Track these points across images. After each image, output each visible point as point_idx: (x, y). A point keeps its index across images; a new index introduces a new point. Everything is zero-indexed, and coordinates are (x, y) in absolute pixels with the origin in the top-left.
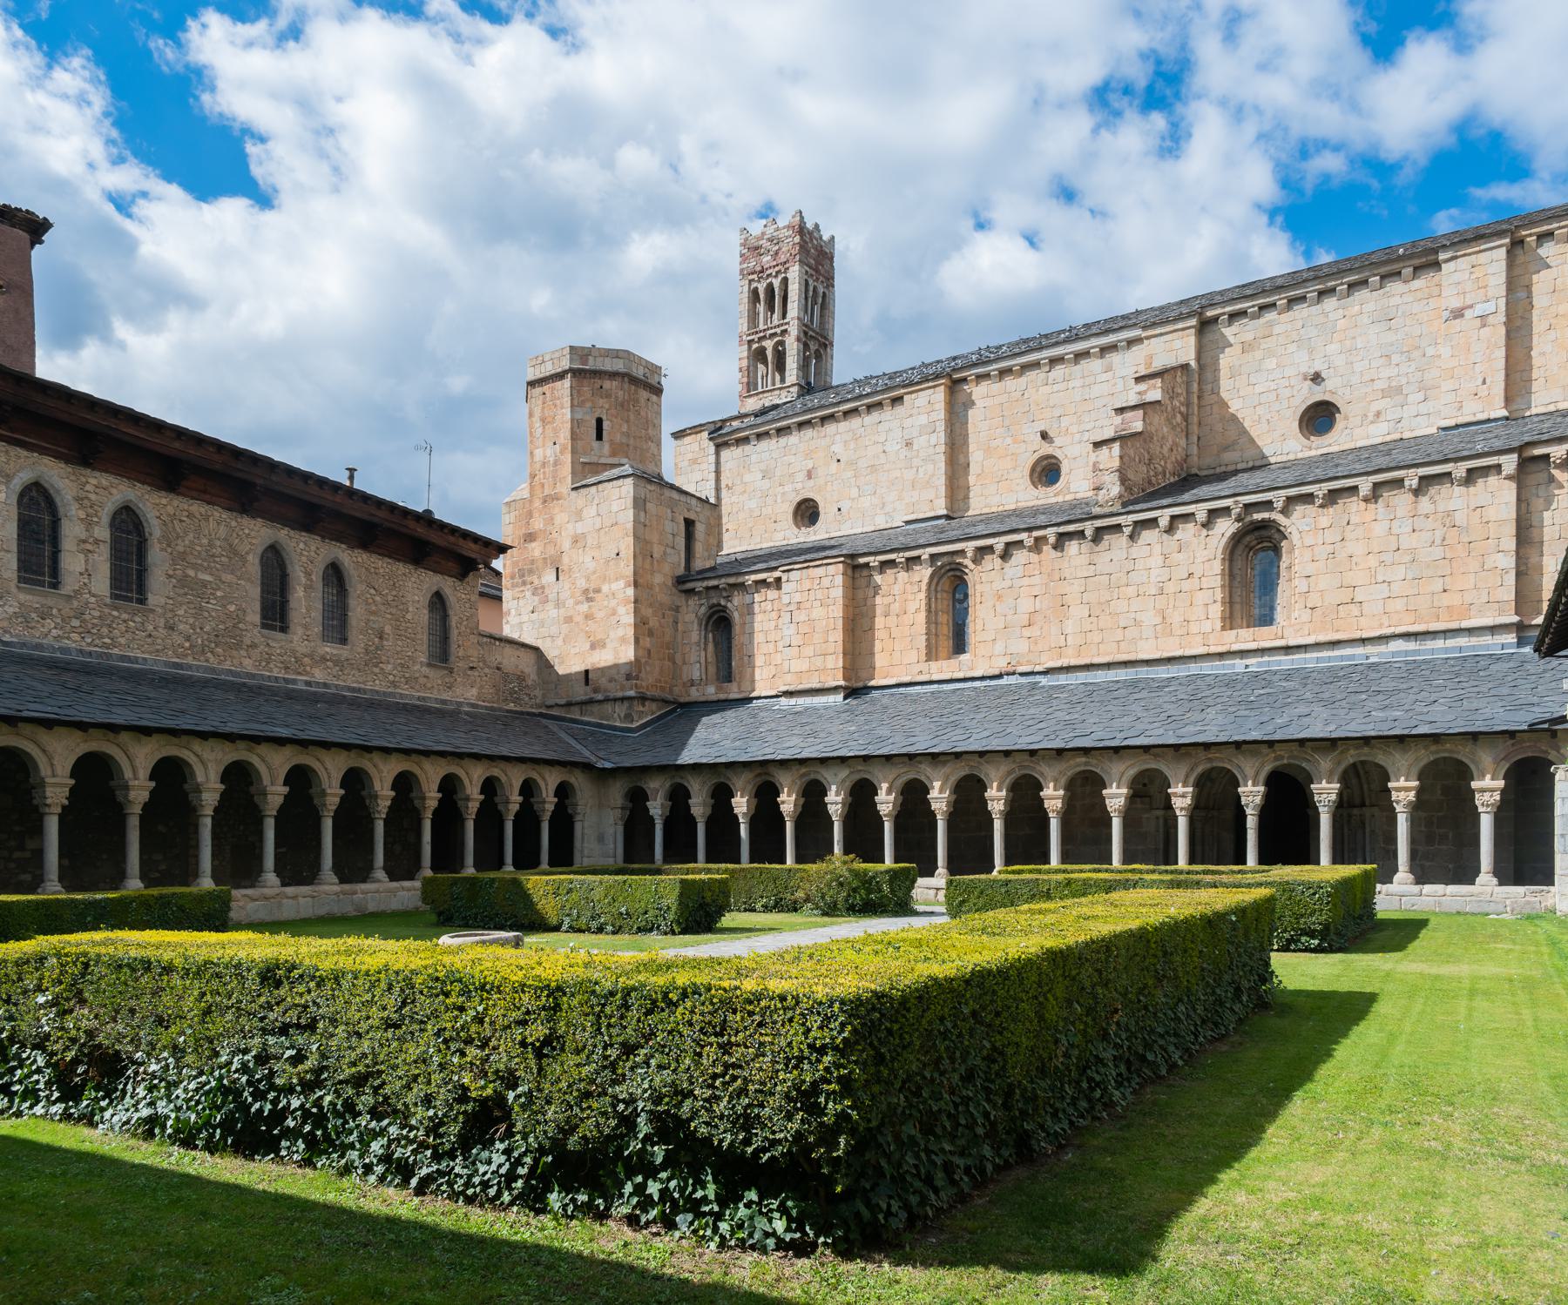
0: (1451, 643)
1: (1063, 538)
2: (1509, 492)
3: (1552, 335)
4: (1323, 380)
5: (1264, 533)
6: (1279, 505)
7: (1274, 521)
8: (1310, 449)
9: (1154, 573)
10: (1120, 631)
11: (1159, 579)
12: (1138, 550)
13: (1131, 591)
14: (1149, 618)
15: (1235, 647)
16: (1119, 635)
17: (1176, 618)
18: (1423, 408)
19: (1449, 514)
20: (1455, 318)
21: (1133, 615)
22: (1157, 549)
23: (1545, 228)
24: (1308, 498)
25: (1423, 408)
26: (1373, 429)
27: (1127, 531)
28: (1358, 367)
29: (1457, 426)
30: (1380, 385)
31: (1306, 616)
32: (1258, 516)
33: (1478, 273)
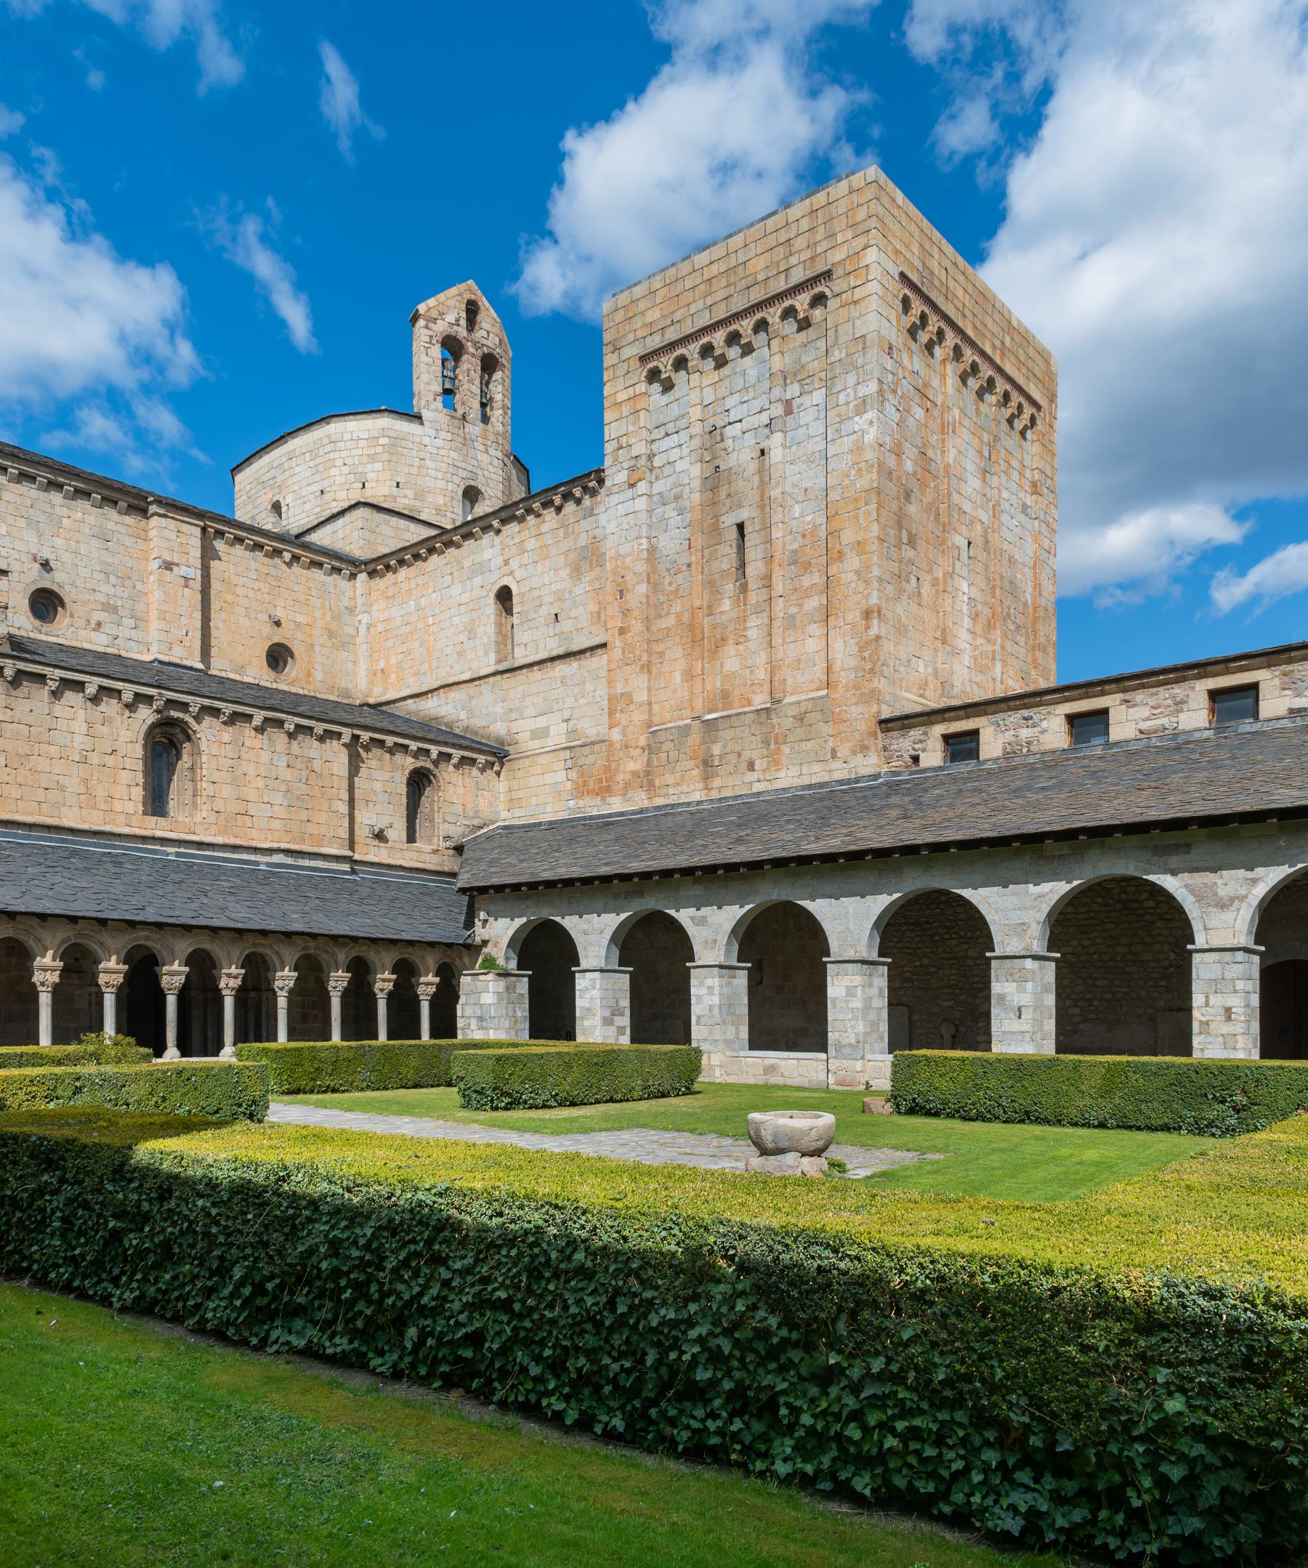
0: (313, 863)
1: (67, 684)
2: (343, 757)
3: (223, 616)
4: (51, 569)
5: (169, 729)
6: (194, 709)
7: (186, 723)
8: (40, 632)
9: (79, 739)
10: (41, 791)
11: (83, 747)
12: (59, 709)
13: (53, 751)
14: (73, 784)
15: (159, 834)
16: (41, 795)
17: (101, 792)
18: (134, 634)
19: (311, 760)
20: (167, 568)
21: (56, 778)
22: (81, 714)
23: (220, 527)
24: (215, 712)
25: (134, 634)
26: (94, 635)
27: (53, 685)
28: (82, 572)
29: (170, 664)
30: (101, 598)
31: (212, 818)
32: (175, 714)
33: (183, 539)
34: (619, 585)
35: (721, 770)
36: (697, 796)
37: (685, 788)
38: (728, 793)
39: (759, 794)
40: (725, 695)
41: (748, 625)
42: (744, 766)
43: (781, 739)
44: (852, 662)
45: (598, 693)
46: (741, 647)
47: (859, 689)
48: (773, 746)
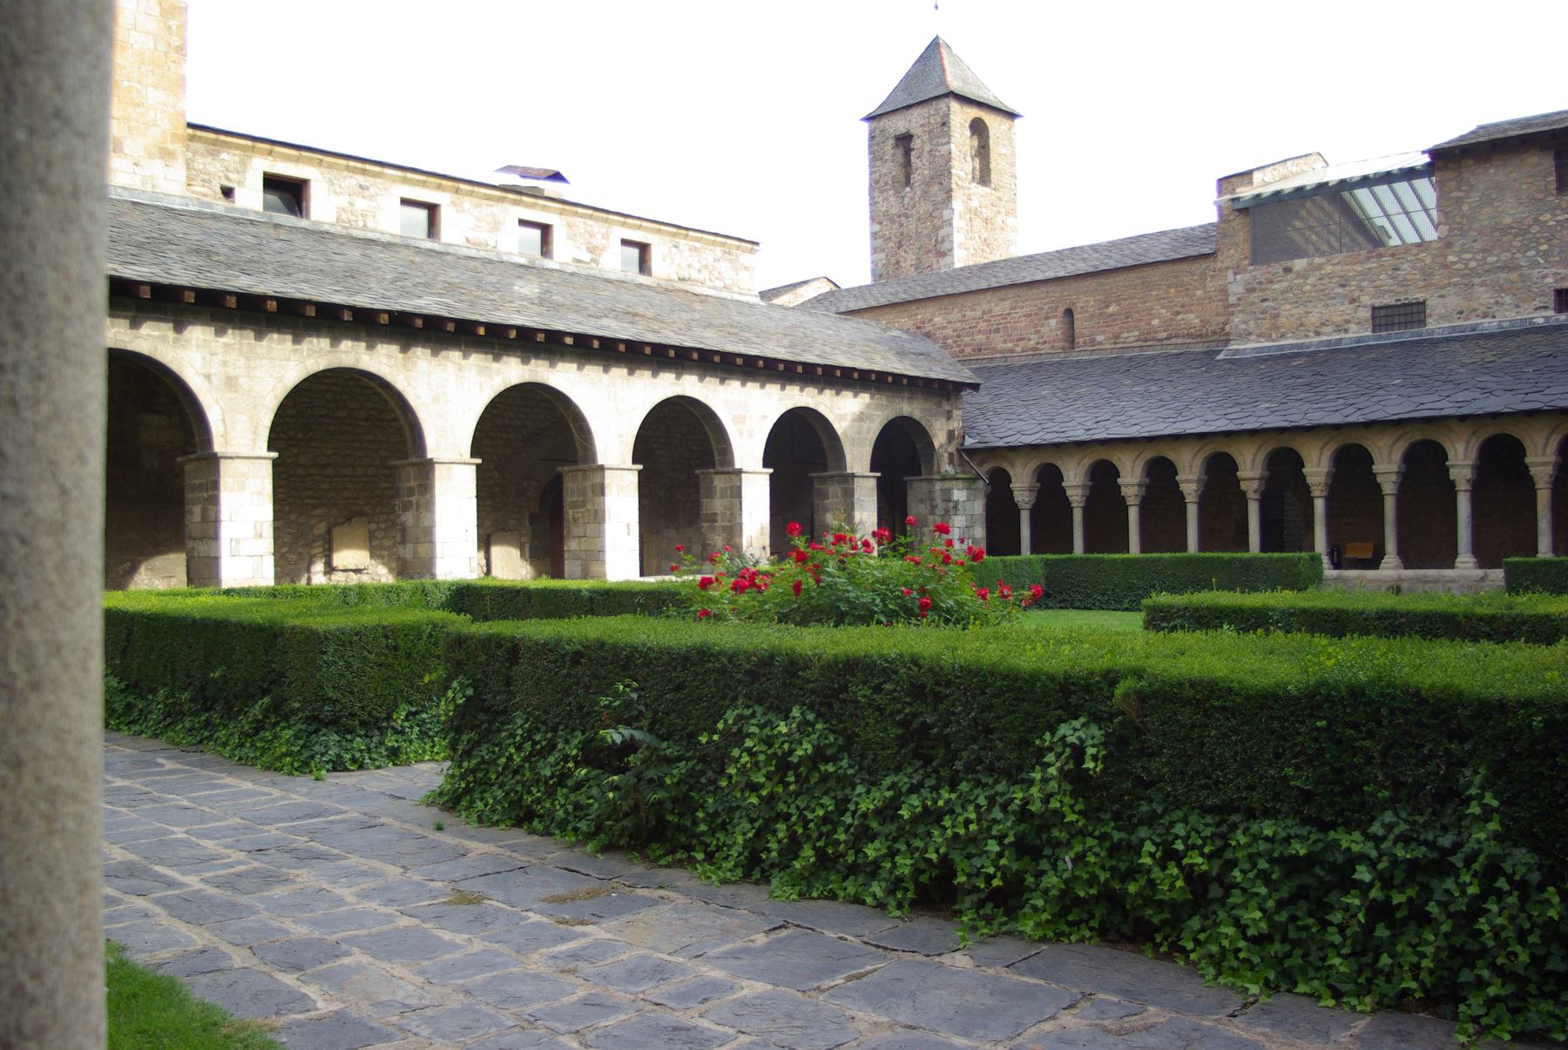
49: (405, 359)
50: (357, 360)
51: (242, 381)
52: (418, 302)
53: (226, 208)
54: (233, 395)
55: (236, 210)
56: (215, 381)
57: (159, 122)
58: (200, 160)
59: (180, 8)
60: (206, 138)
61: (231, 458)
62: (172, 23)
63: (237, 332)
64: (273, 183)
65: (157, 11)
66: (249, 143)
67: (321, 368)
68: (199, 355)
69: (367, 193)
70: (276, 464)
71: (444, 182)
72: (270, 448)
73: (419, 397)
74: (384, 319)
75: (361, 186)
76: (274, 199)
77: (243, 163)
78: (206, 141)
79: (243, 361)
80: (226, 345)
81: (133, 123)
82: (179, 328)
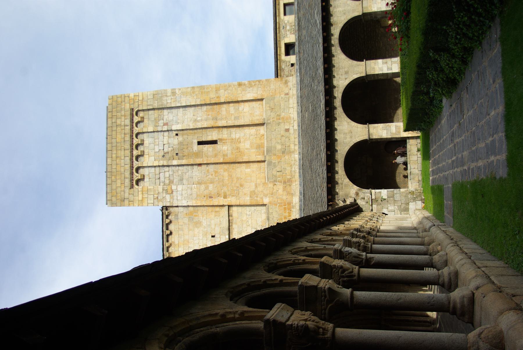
34: (207, 198)
35: (288, 144)
36: (297, 156)
37: (293, 162)
38: (297, 140)
39: (299, 126)
40: (259, 147)
41: (234, 137)
42: (287, 134)
43: (278, 117)
44: (255, 89)
45: (248, 213)
46: (242, 140)
47: (265, 86)
48: (281, 121)
49: (334, 25)
50: (336, 38)
51: (346, 70)
52: (318, 22)
53: (297, 65)
54: (350, 72)
55: (297, 63)
56: (347, 77)
57: (279, 85)
58: (285, 73)
59: (249, 83)
60: (280, 72)
61: (366, 72)
62: (253, 85)
63: (333, 72)
64: (287, 54)
65: (251, 88)
66: (278, 61)
67: (340, 49)
68: (340, 82)
69: (285, 26)
70: (366, 60)
71: (277, 4)
72: (363, 61)
73: (344, 19)
74: (325, 34)
75: (283, 28)
76: (291, 52)
77: (284, 62)
78: (280, 72)
79: (341, 70)
80: (337, 75)
81: (280, 91)
82: (335, 87)
